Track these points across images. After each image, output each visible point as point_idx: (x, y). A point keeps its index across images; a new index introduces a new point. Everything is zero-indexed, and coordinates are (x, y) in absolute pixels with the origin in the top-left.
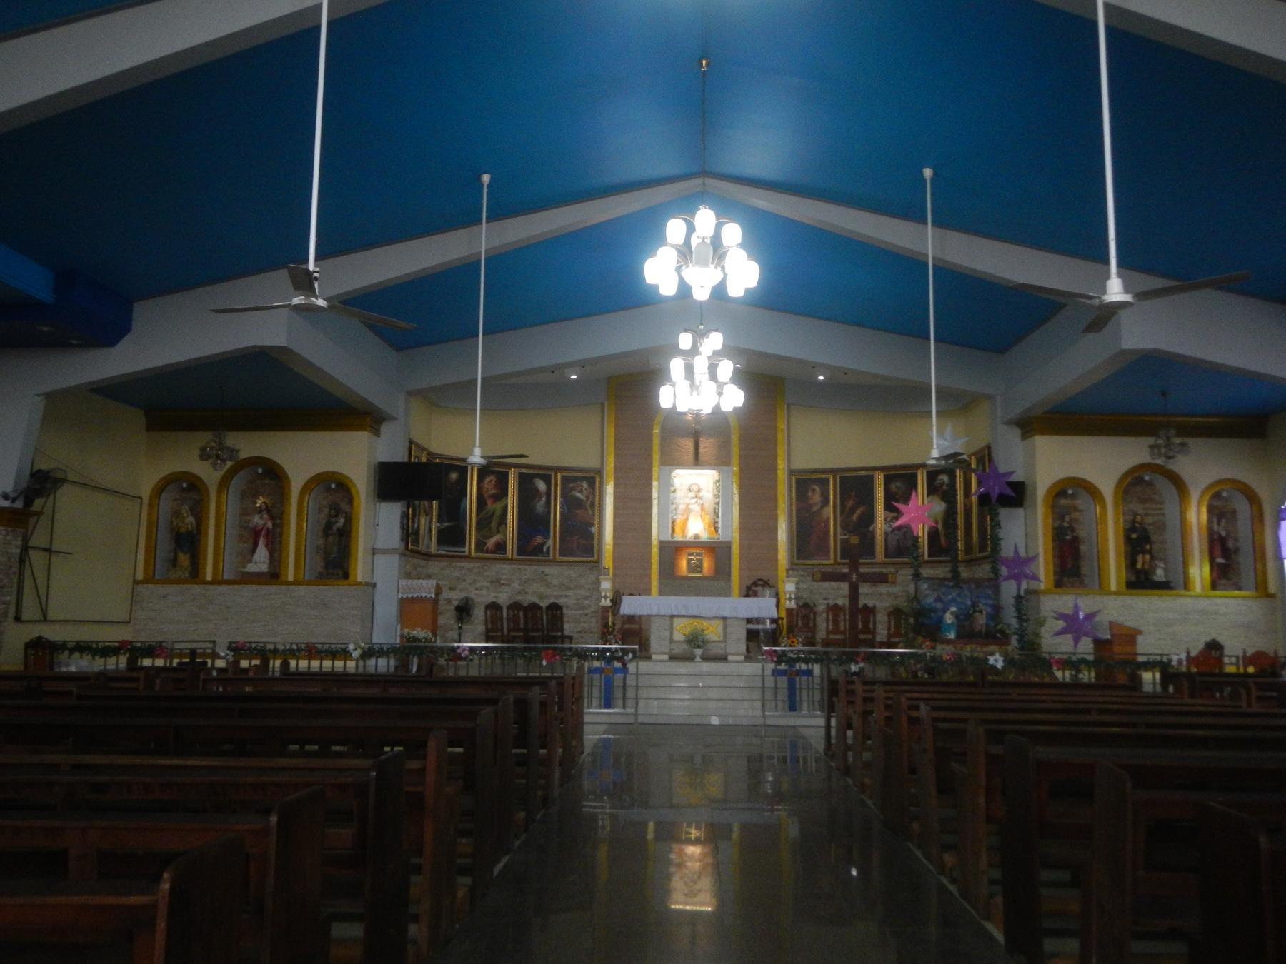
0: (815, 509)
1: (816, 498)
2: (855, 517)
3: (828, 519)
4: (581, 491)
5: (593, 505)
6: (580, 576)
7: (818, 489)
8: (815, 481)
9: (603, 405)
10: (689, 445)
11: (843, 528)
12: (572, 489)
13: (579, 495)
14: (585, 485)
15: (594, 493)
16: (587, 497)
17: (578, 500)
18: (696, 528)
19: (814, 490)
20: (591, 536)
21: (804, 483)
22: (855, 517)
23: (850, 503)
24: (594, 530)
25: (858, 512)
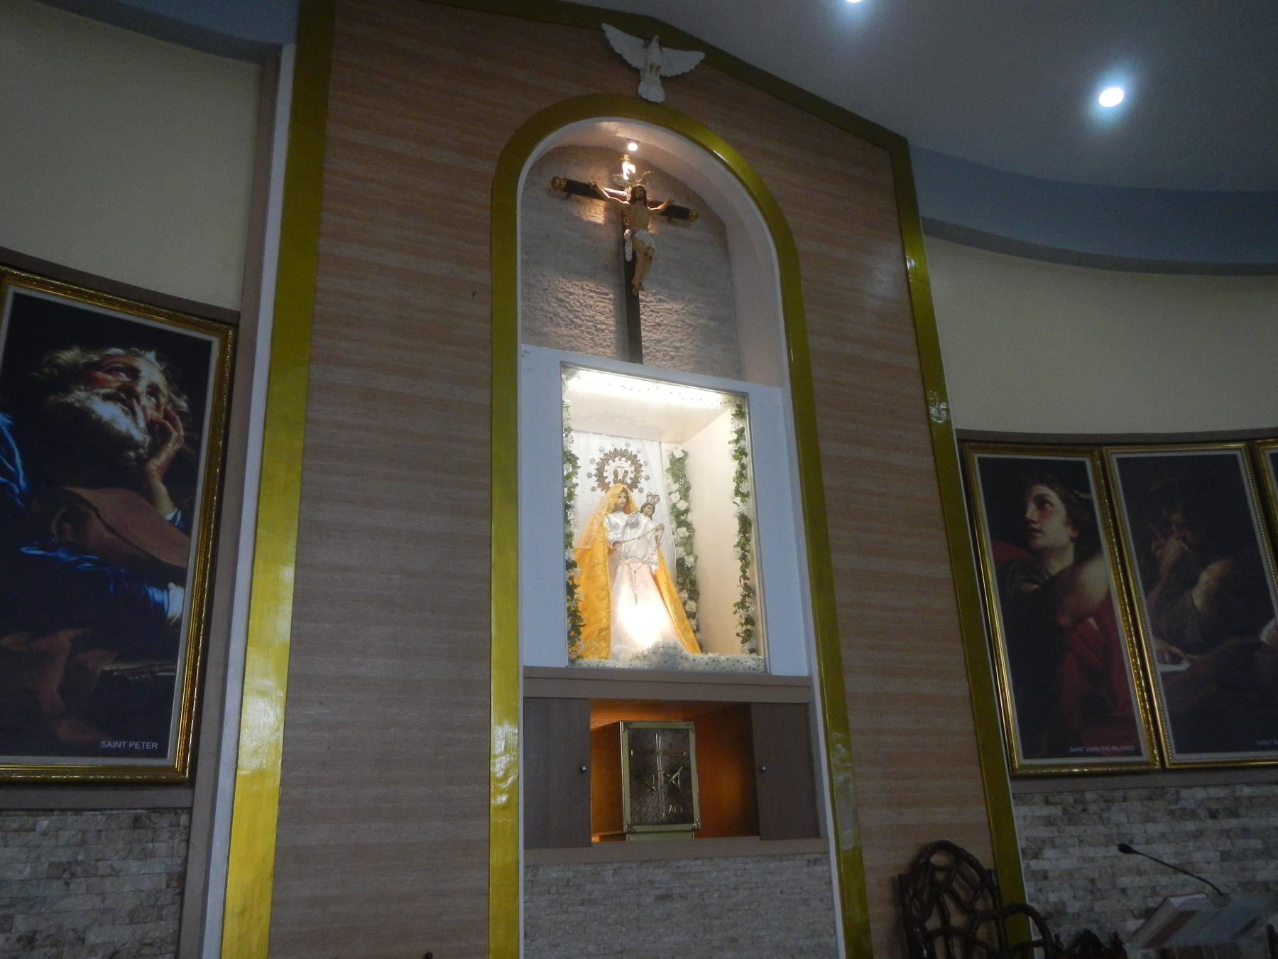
0: (1057, 566)
1: (1055, 528)
2: (1197, 597)
3: (1108, 596)
4: (126, 397)
5: (180, 475)
6: (65, 872)
7: (1053, 496)
8: (1045, 472)
9: (266, 59)
10: (596, 304)
11: (1158, 634)
12: (85, 376)
13: (109, 412)
14: (150, 370)
15: (193, 421)
16: (158, 431)
17: (101, 430)
18: (641, 623)
19: (1042, 502)
20: (163, 637)
21: (1009, 476)
22: (1197, 597)
23: (1172, 549)
24: (177, 601)
25: (1204, 577)
